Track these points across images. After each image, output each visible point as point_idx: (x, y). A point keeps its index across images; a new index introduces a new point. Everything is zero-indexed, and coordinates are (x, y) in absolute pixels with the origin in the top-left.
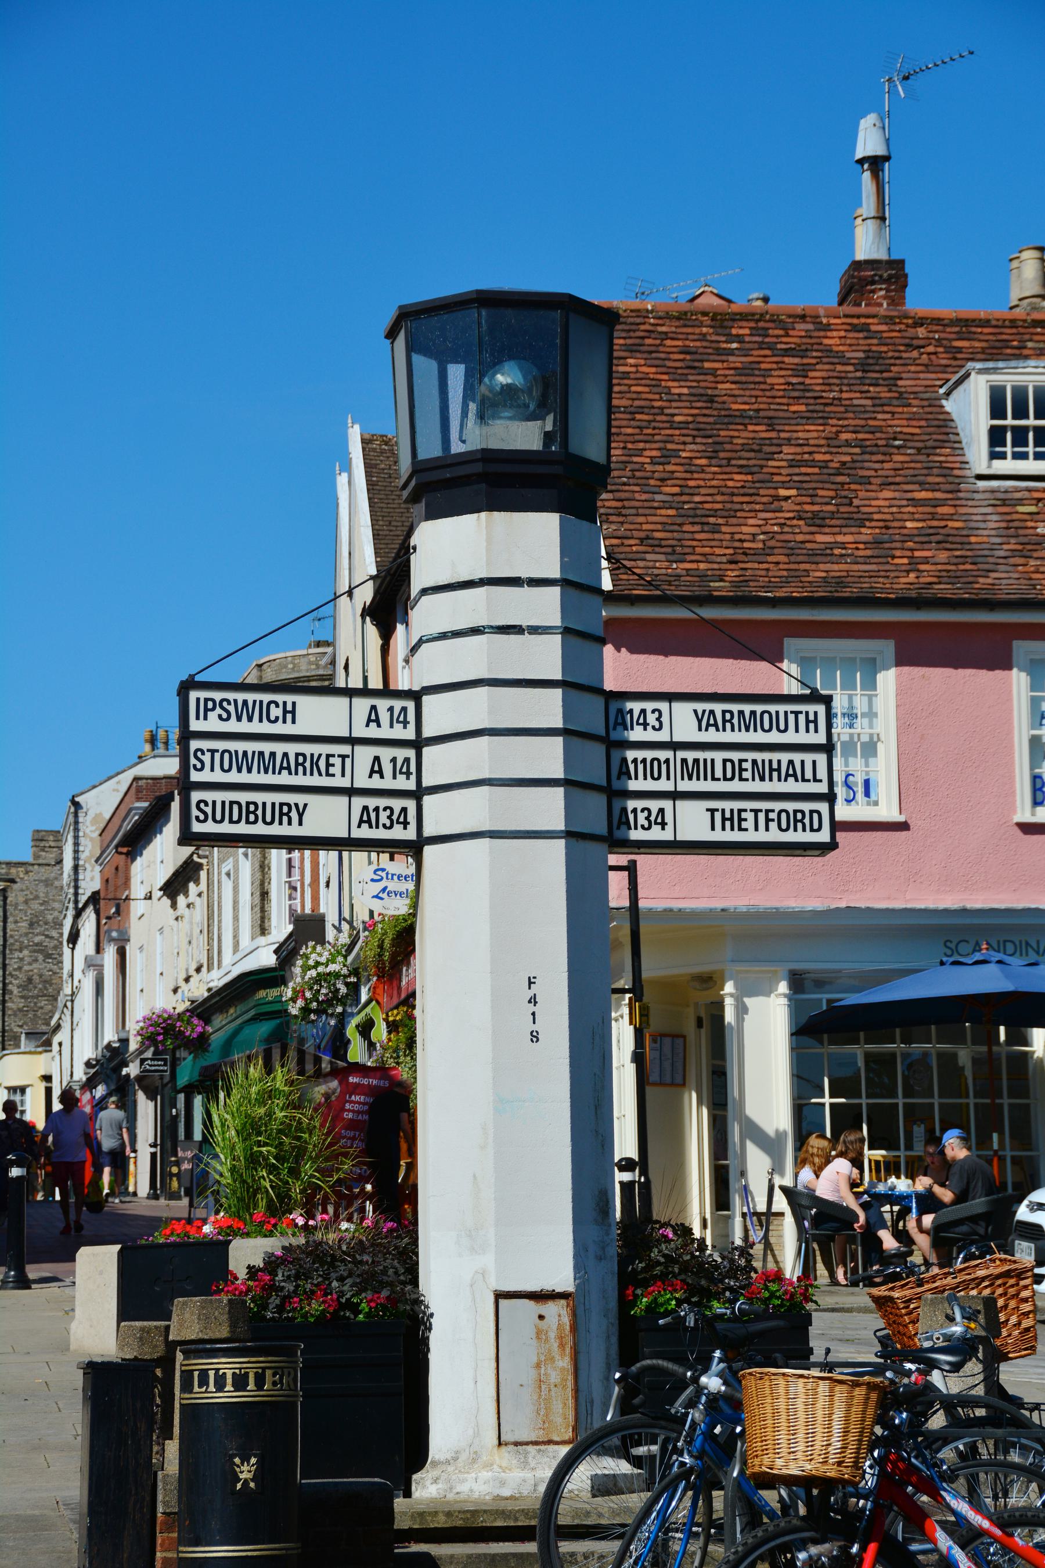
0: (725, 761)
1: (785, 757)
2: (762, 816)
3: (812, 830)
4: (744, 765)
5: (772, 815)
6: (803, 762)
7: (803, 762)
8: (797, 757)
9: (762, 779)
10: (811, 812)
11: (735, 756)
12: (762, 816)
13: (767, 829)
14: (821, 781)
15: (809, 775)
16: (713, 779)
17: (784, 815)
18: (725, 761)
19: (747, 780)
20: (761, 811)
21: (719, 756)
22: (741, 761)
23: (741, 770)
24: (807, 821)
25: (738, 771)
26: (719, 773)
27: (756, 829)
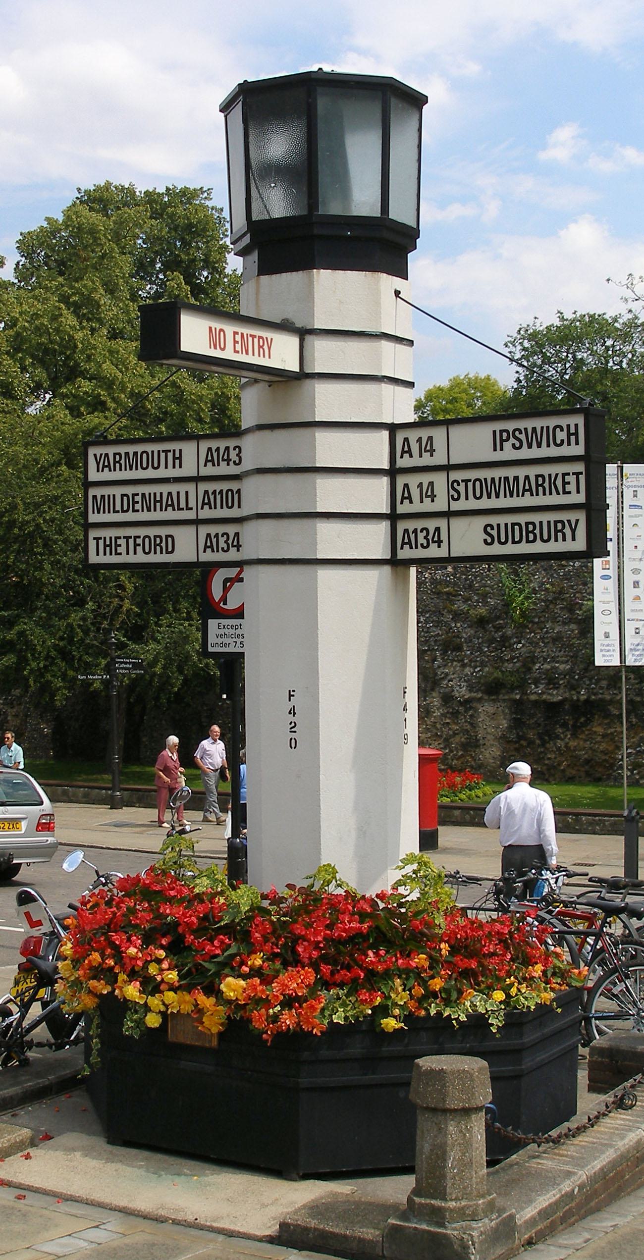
0: (123, 496)
1: (165, 489)
2: (131, 541)
3: (167, 552)
4: (137, 499)
5: (139, 541)
6: (178, 493)
7: (178, 493)
8: (174, 488)
9: (149, 510)
10: (167, 537)
11: (129, 490)
12: (131, 541)
13: (135, 553)
14: (191, 509)
15: (183, 504)
16: (115, 511)
17: (147, 540)
18: (123, 496)
19: (138, 511)
20: (131, 537)
21: (118, 491)
22: (134, 495)
23: (135, 503)
24: (163, 545)
25: (130, 503)
26: (118, 508)
27: (128, 553)
